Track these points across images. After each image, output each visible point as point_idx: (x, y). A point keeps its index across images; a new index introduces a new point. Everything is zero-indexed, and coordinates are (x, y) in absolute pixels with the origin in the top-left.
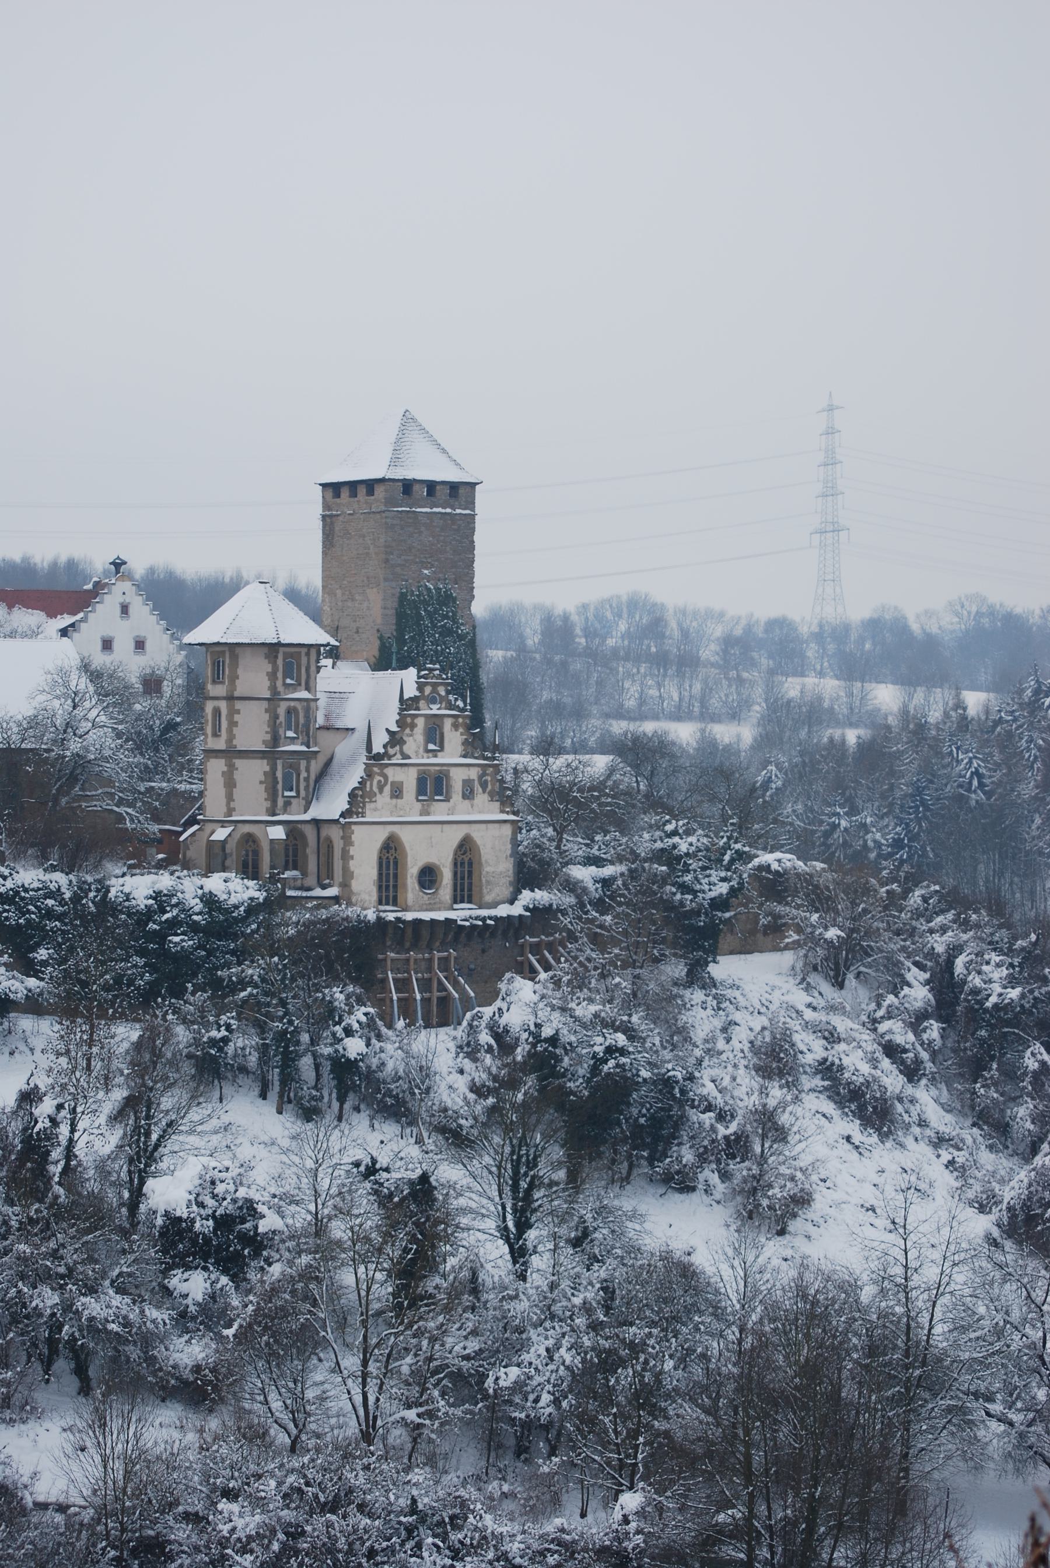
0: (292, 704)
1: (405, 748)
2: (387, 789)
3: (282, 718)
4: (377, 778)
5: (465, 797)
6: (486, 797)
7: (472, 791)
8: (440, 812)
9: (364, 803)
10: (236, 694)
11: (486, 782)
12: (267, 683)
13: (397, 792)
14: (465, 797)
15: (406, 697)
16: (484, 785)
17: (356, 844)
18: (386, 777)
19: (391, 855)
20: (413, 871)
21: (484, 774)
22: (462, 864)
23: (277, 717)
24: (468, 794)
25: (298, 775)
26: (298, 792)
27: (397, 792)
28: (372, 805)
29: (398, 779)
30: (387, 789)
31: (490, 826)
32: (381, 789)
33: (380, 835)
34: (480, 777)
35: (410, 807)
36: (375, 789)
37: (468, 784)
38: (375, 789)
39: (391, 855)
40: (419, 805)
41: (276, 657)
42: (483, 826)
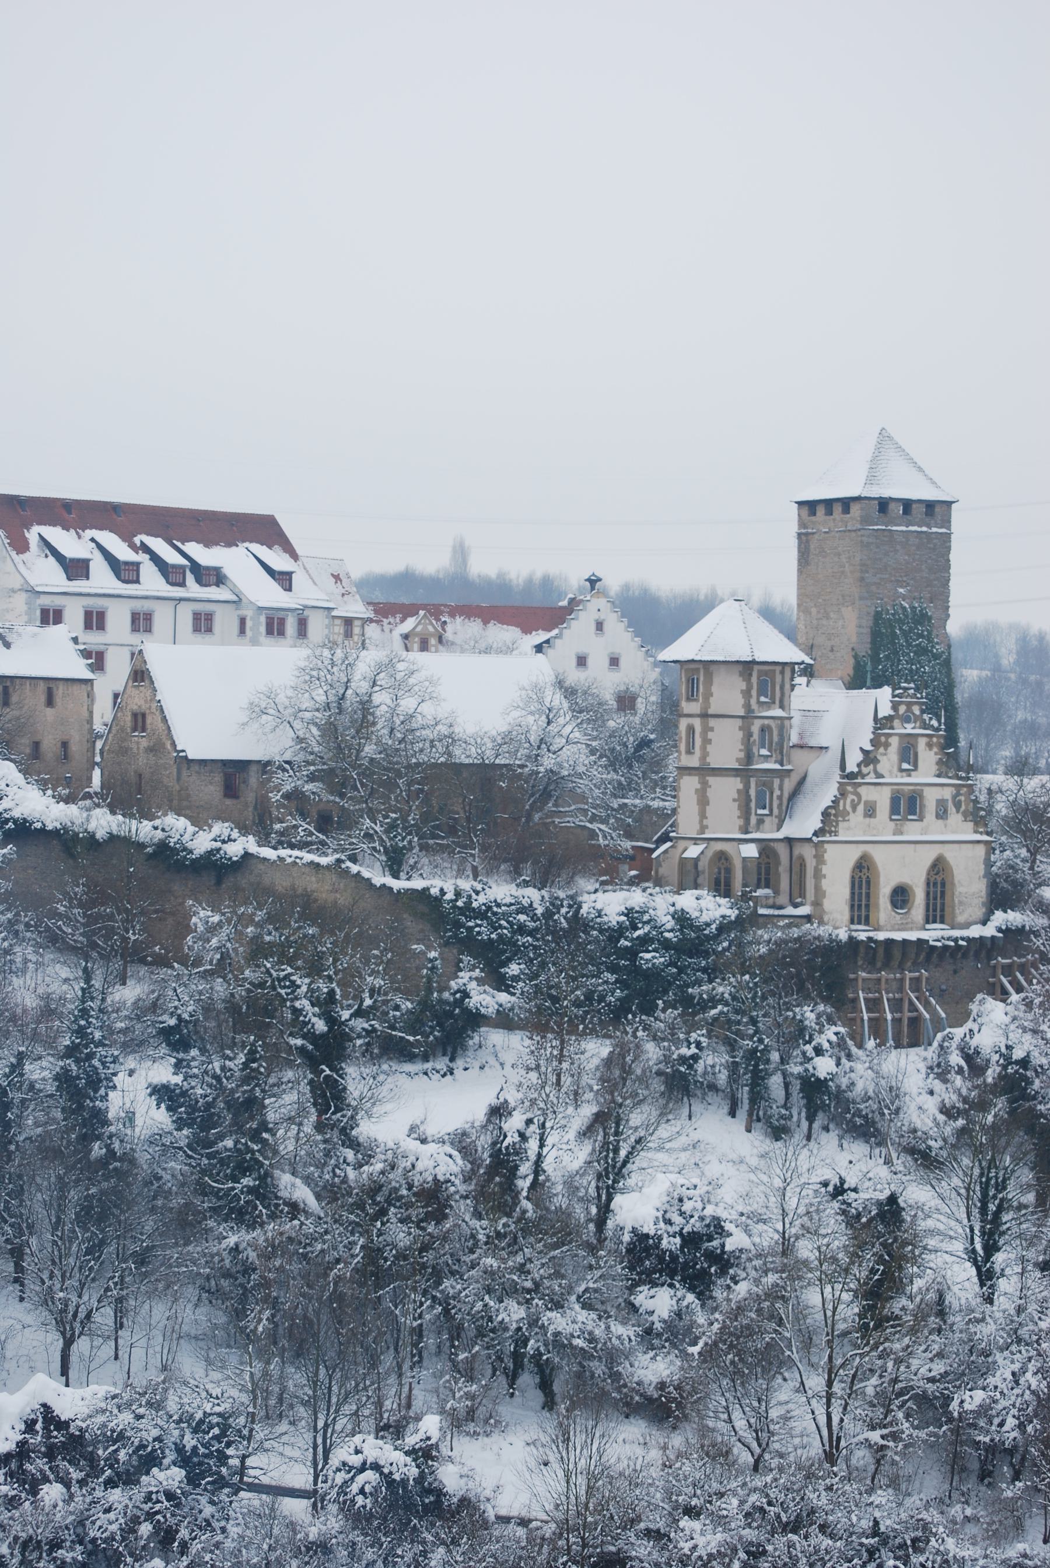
0: (766, 722)
1: (879, 767)
2: (861, 808)
3: (756, 736)
4: (850, 797)
5: (938, 816)
6: (960, 817)
7: (946, 811)
8: (913, 831)
9: (837, 822)
10: (710, 712)
12: (742, 701)
13: (870, 811)
14: (938, 816)
15: (880, 716)
16: (958, 805)
18: (859, 796)
19: (863, 875)
20: (884, 891)
21: (958, 794)
22: (935, 884)
23: (750, 735)
24: (942, 814)
25: (772, 793)
26: (771, 810)
27: (870, 811)
28: (845, 824)
29: (871, 798)
30: (861, 808)
31: (964, 846)
32: (854, 808)
33: (853, 854)
34: (954, 797)
35: (883, 826)
36: (849, 808)
37: (941, 804)
38: (849, 808)
39: (863, 875)
40: (892, 824)
41: (750, 675)
42: (956, 846)
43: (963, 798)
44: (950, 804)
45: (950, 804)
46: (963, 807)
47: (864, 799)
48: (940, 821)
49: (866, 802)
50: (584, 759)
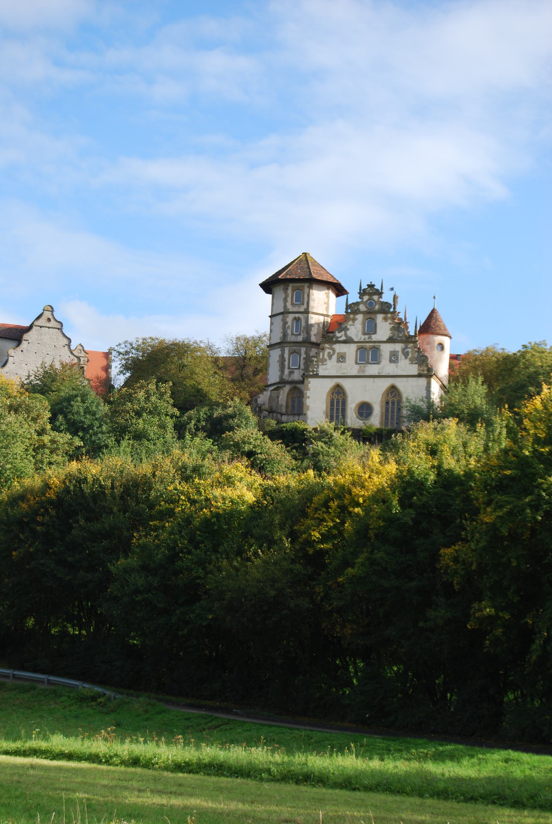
0: (297, 315)
1: (349, 333)
2: (335, 357)
3: (290, 324)
5: (391, 361)
6: (407, 361)
7: (397, 358)
8: (372, 369)
9: (318, 366)
10: (281, 317)
11: (408, 352)
12: (283, 305)
14: (391, 361)
16: (406, 355)
17: (311, 389)
18: (334, 350)
19: (338, 397)
20: (52, 319)
23: (286, 323)
24: (394, 358)
25: (300, 356)
26: (300, 366)
27: (342, 358)
28: (324, 367)
29: (342, 351)
30: (335, 357)
32: (330, 357)
33: (330, 384)
34: (403, 350)
36: (326, 357)
38: (326, 357)
39: (338, 397)
41: (287, 289)
43: (410, 350)
44: (400, 354)
45: (400, 354)
46: (410, 355)
47: (337, 351)
48: (393, 364)
49: (338, 354)
50: (425, 407)
